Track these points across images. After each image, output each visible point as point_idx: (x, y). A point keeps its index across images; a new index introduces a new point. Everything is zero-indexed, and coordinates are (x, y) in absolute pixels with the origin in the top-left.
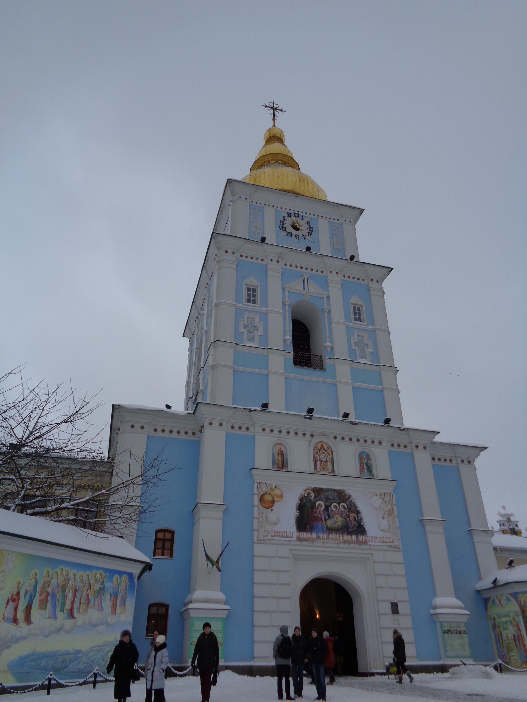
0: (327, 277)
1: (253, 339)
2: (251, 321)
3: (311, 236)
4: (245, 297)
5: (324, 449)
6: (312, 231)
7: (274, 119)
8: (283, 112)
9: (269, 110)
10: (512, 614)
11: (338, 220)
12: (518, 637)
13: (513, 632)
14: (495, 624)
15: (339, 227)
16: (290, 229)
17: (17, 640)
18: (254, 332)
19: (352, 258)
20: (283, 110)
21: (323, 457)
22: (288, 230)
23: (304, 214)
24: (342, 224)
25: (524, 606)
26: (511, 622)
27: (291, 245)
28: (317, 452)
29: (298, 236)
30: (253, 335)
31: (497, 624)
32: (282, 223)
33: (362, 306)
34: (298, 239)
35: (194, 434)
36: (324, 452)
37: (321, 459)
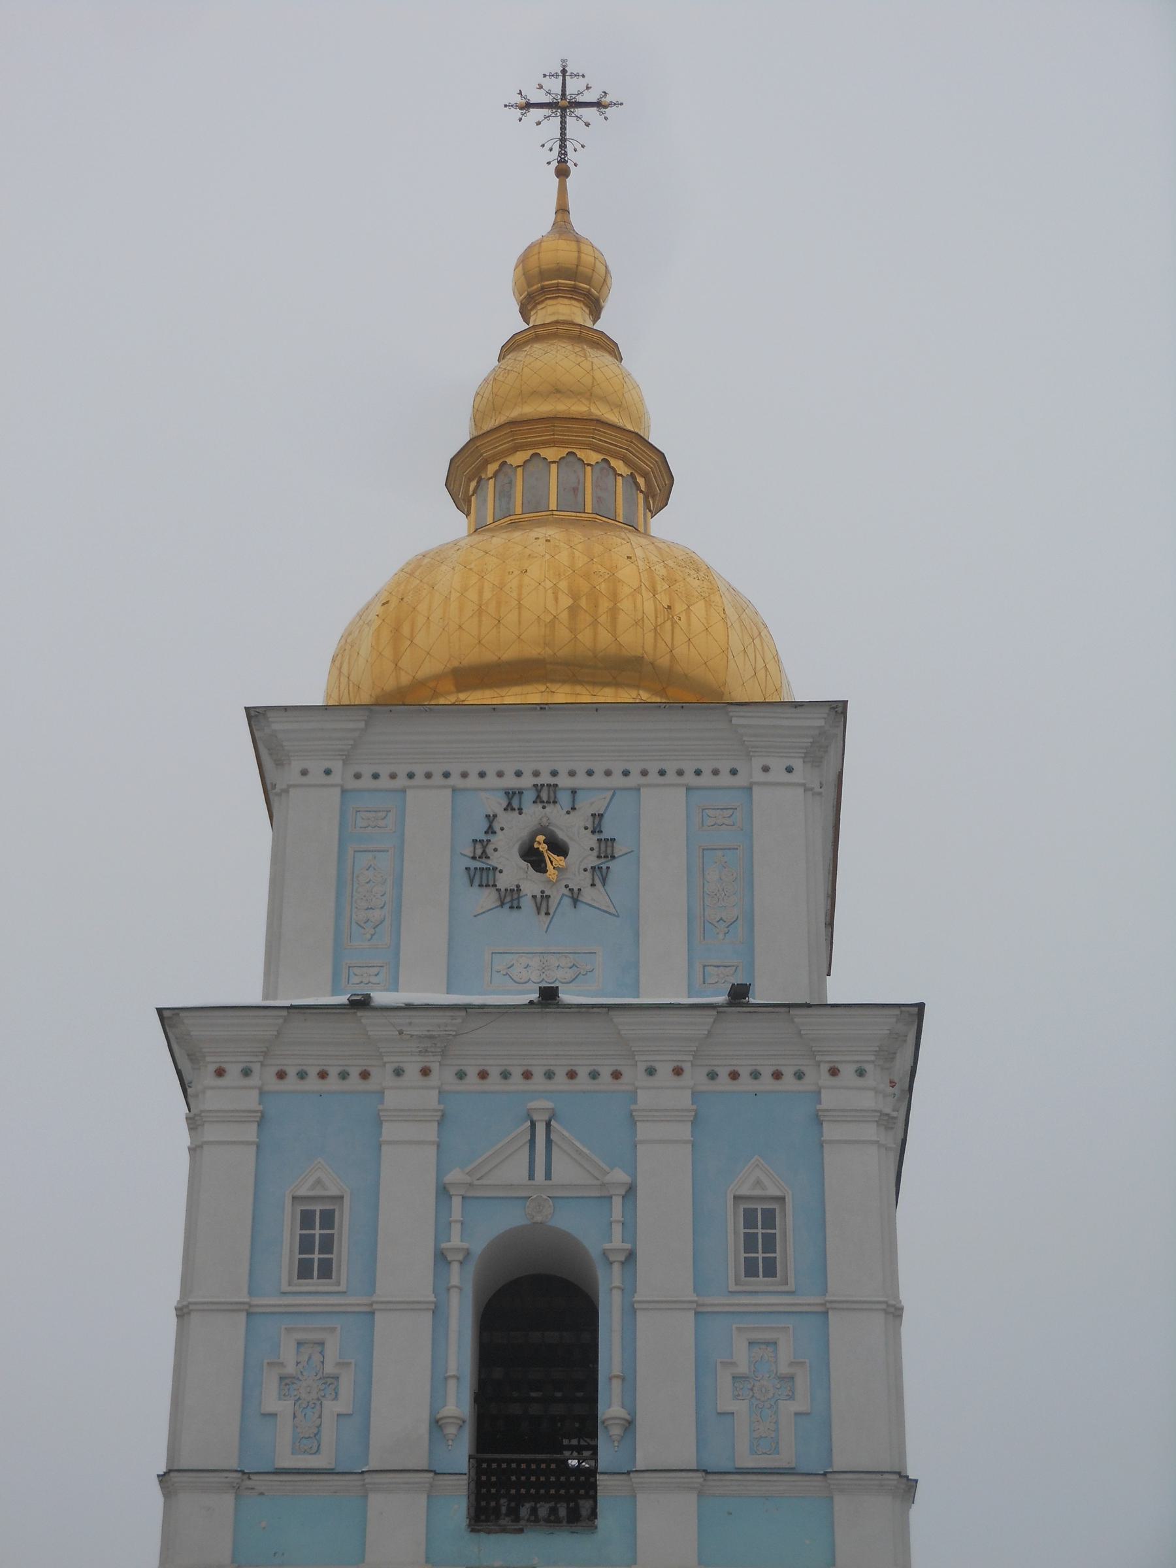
0: (633, 1096)
1: (315, 1435)
2: (310, 1358)
6: (613, 857)
7: (562, 172)
8: (609, 111)
9: (538, 123)
11: (734, 772)
18: (321, 1404)
19: (739, 994)
22: (505, 881)
23: (580, 781)
24: (749, 789)
30: (317, 1415)
32: (479, 852)
33: (781, 1199)
34: (547, 914)
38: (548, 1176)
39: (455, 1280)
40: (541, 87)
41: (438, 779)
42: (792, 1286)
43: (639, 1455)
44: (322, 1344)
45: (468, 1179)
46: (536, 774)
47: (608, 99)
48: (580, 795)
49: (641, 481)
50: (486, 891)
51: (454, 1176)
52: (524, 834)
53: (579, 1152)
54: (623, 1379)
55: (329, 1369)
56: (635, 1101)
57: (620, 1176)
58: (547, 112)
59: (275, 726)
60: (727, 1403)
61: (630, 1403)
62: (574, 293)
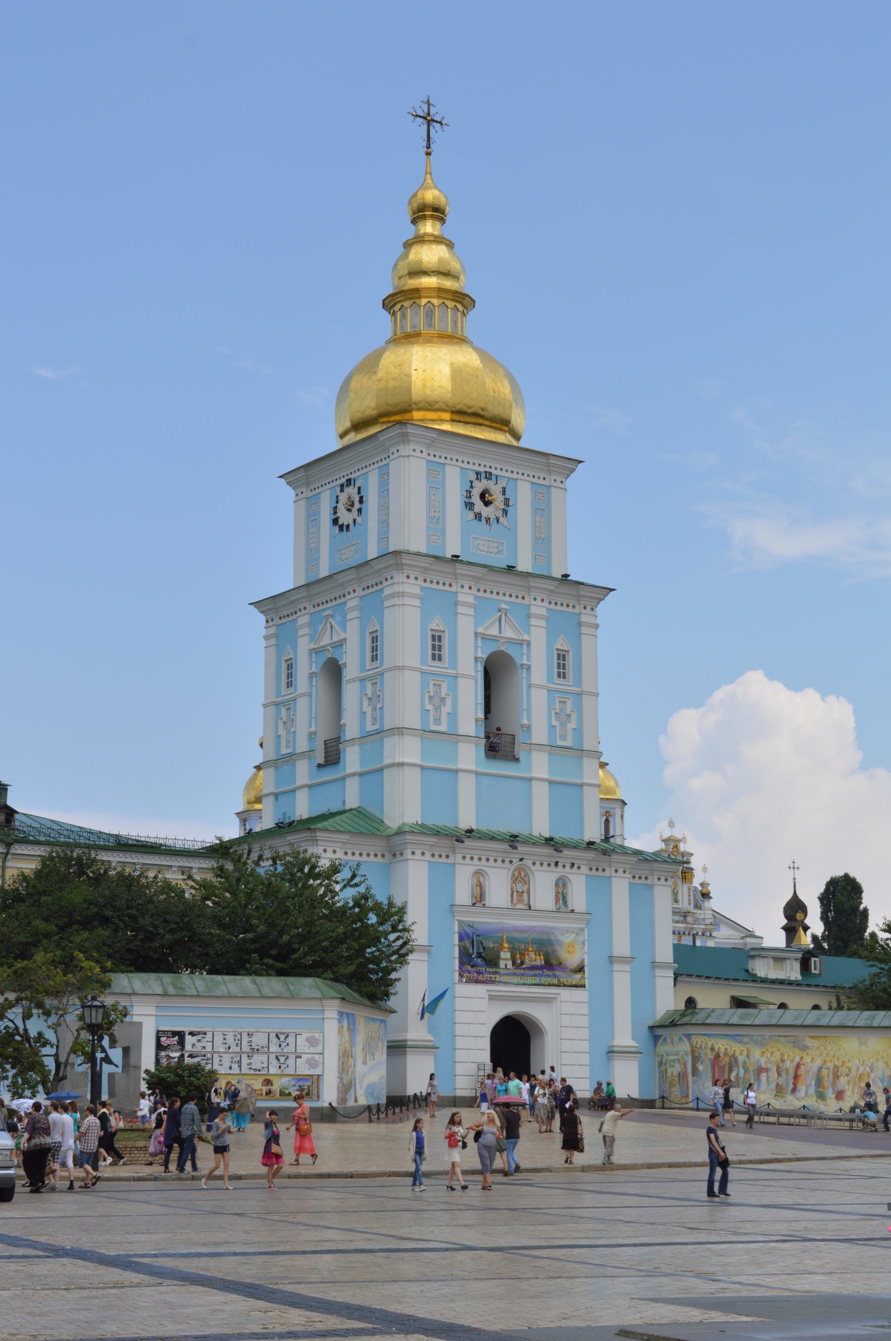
4: (430, 652)
7: (428, 154)
10: (682, 1053)
11: (544, 479)
12: (683, 1074)
13: (679, 1070)
14: (662, 1061)
16: (479, 506)
17: (365, 1075)
20: (443, 123)
23: (498, 472)
25: (695, 1047)
26: (679, 1060)
31: (664, 1061)
33: (568, 651)
35: (383, 856)
41: (454, 462)
42: (571, 684)
44: (440, 685)
46: (485, 466)
50: (471, 512)
51: (481, 630)
52: (481, 491)
55: (443, 695)
57: (526, 637)
58: (422, 120)
59: (409, 430)
60: (555, 723)
61: (529, 717)
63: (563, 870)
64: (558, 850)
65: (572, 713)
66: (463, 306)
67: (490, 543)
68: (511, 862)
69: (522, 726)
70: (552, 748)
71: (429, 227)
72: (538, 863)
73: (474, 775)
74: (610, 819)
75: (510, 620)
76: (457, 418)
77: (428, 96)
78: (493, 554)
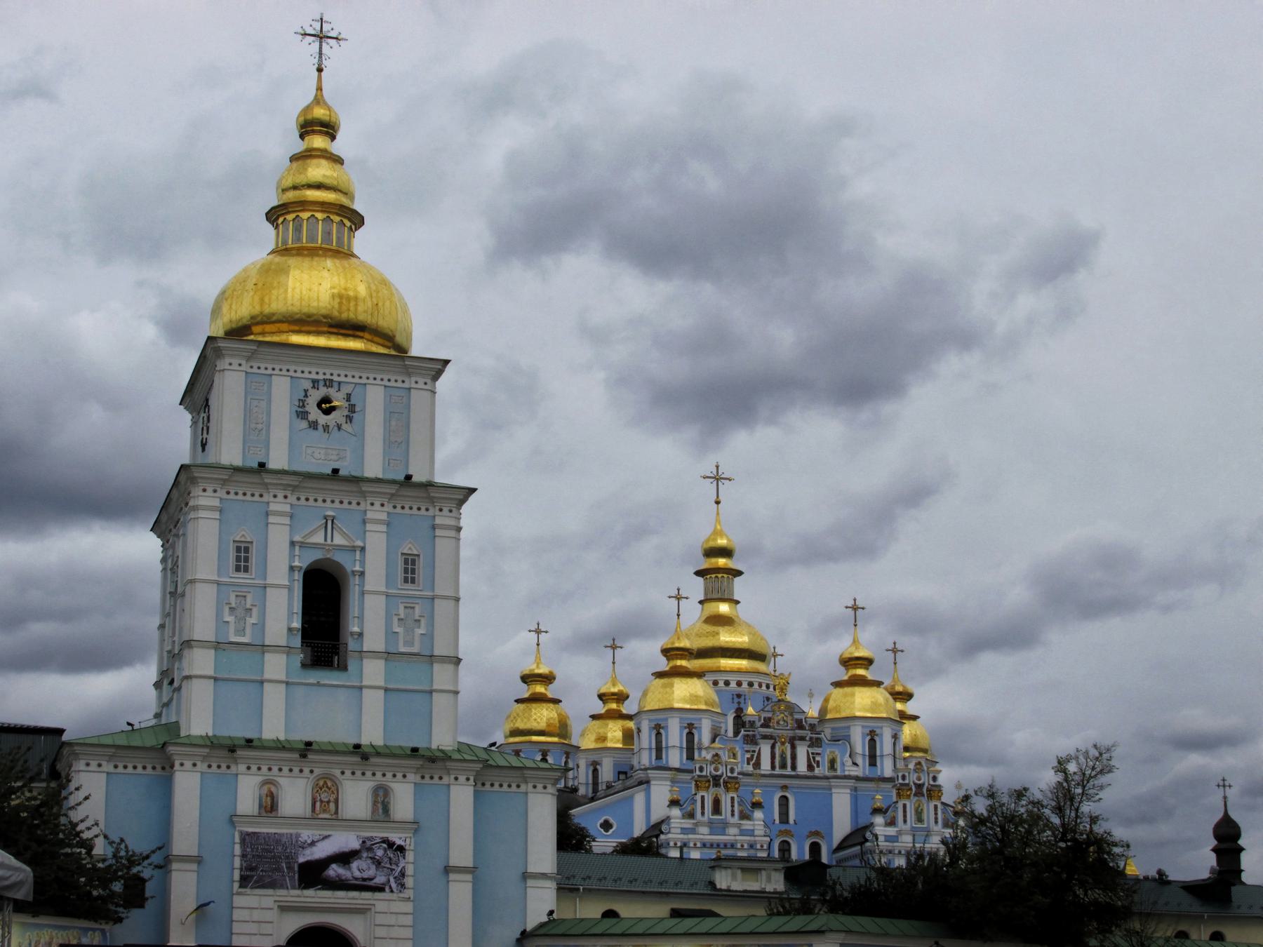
0: (365, 512)
3: (351, 422)
5: (327, 787)
7: (320, 70)
8: (341, 42)
9: (310, 44)
15: (403, 397)
16: (315, 414)
21: (324, 797)
22: (311, 417)
23: (342, 379)
27: (315, 446)
28: (318, 791)
29: (328, 426)
32: (301, 404)
36: (327, 790)
37: (322, 799)
38: (332, 541)
39: (296, 578)
40: (311, 26)
41: (284, 372)
43: (365, 645)
45: (302, 540)
46: (324, 374)
47: (340, 38)
48: (342, 384)
49: (353, 227)
50: (304, 421)
51: (297, 538)
53: (345, 533)
54: (358, 617)
56: (366, 515)
57: (359, 543)
58: (313, 38)
61: (361, 625)
62: (327, 134)
63: (384, 779)
64: (365, 757)
65: (417, 618)
66: (338, 215)
67: (330, 451)
68: (312, 772)
69: (352, 634)
70: (388, 655)
71: (318, 142)
72: (348, 773)
73: (284, 686)
74: (876, 738)
75: (338, 526)
76: (297, 328)
77: (322, 14)
78: (331, 462)
